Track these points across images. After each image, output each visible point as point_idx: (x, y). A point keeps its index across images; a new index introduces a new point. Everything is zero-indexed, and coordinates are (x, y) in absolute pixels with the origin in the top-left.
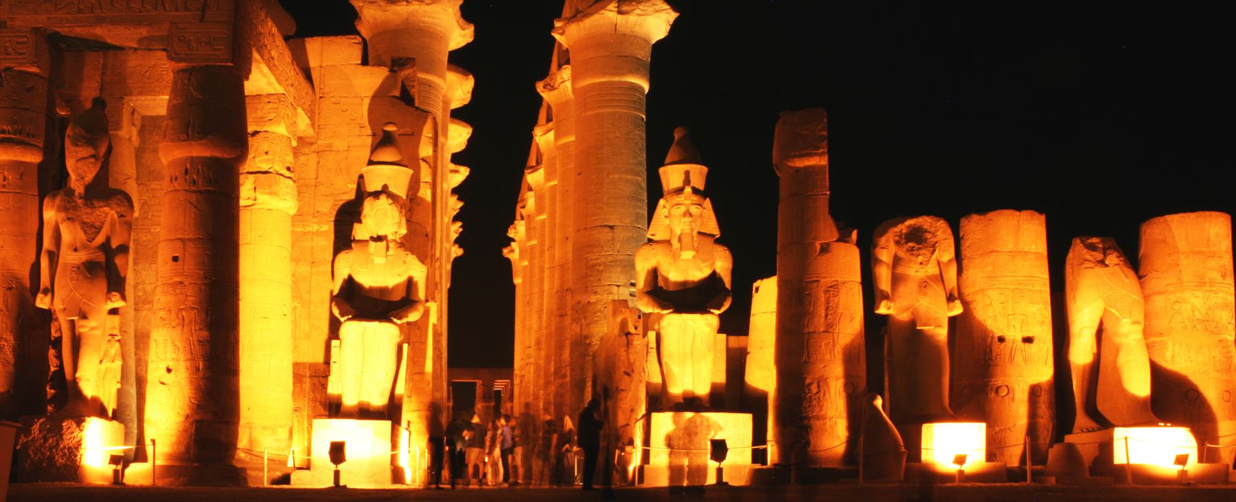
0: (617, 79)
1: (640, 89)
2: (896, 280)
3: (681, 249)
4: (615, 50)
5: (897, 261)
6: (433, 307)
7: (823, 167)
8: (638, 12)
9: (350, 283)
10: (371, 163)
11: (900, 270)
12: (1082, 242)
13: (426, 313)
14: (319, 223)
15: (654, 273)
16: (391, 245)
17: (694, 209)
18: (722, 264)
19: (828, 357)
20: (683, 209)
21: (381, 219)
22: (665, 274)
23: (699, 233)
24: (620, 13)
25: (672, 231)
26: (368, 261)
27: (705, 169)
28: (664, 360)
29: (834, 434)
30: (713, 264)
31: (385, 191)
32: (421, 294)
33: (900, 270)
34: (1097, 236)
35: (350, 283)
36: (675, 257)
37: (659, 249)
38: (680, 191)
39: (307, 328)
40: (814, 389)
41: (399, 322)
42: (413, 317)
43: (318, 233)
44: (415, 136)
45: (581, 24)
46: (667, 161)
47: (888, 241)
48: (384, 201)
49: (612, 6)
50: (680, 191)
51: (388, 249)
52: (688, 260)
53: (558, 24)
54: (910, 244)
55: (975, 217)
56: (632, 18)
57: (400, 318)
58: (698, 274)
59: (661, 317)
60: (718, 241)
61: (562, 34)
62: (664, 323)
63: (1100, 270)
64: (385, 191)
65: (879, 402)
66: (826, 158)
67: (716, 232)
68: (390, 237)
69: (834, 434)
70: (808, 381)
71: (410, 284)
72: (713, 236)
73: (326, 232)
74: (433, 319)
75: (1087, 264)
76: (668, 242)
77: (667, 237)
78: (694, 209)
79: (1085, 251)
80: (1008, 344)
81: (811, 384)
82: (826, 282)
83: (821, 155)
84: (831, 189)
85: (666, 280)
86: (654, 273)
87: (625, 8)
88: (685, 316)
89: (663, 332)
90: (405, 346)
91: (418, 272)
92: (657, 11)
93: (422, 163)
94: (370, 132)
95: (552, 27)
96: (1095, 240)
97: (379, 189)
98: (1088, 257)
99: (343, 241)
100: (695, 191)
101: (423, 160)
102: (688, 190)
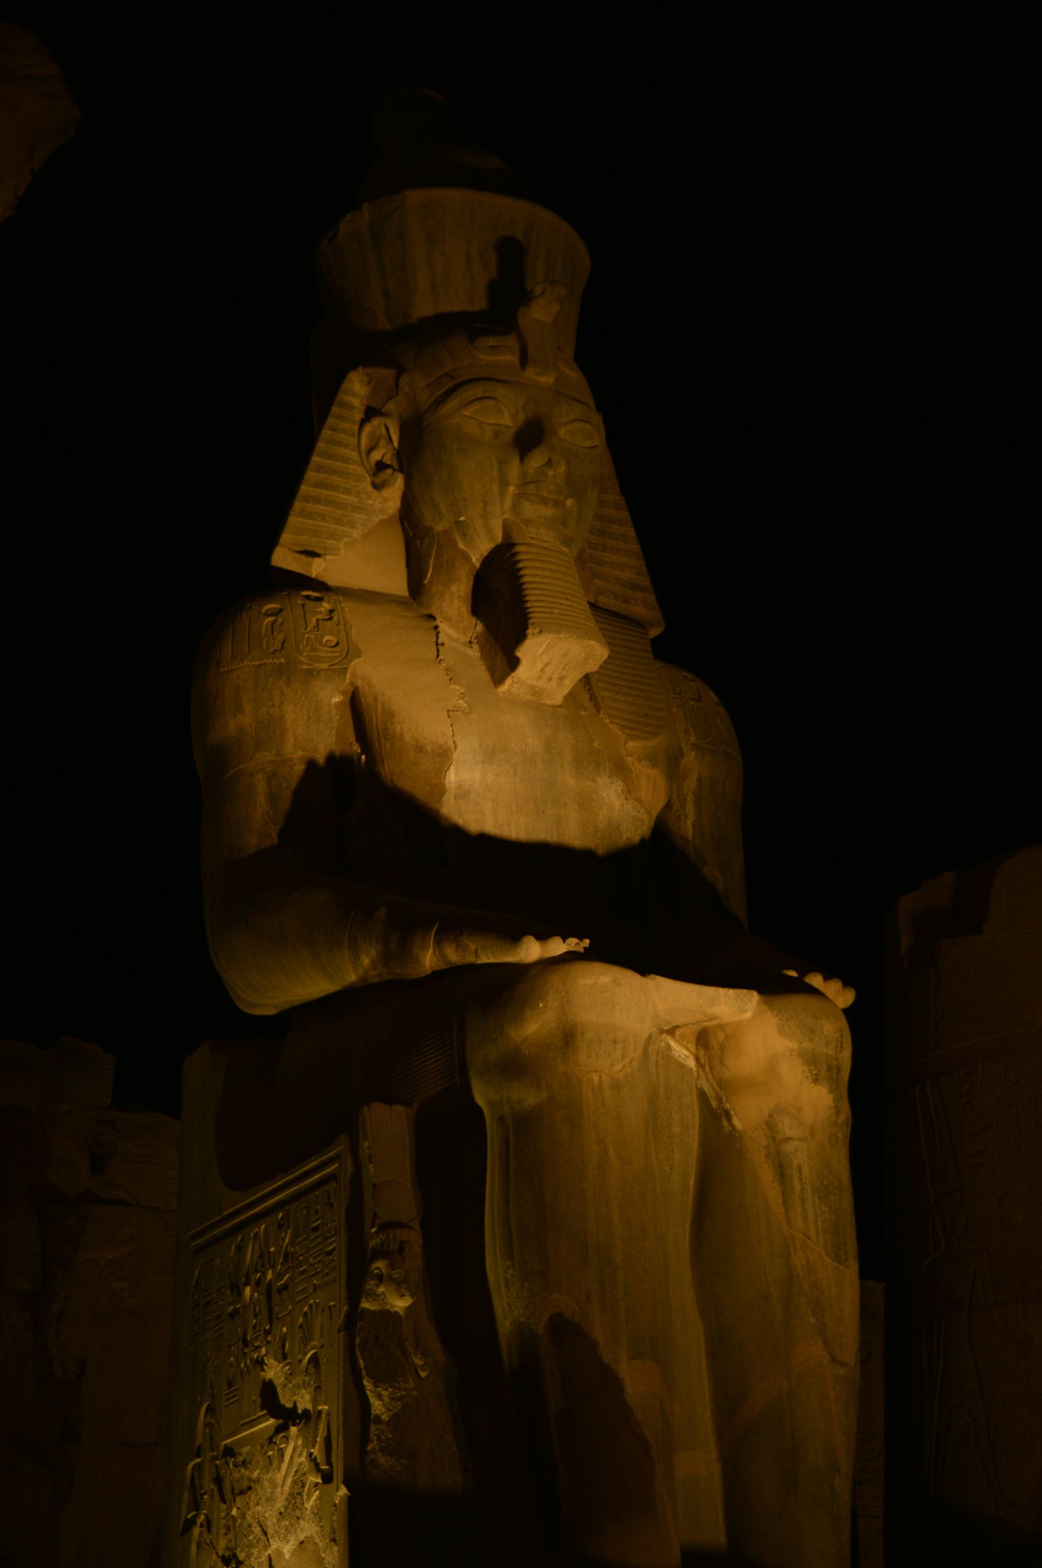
60: (664, 650)
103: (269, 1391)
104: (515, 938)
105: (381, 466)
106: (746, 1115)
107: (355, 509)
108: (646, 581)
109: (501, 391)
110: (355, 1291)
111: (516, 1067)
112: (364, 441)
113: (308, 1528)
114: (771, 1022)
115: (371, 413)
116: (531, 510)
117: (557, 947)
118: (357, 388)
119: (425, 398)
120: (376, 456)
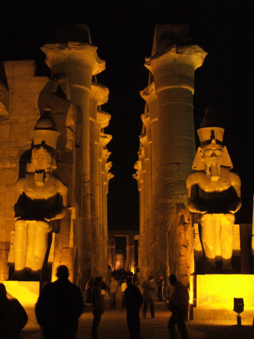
0: (177, 87)
1: (190, 92)
3: (211, 175)
4: (175, 72)
6: (73, 210)
8: (187, 52)
9: (23, 198)
10: (36, 129)
13: (70, 213)
14: (11, 163)
16: (47, 175)
17: (217, 153)
18: (235, 182)
20: (211, 152)
21: (41, 161)
22: (203, 189)
23: (221, 166)
24: (177, 53)
26: (33, 186)
27: (223, 130)
28: (204, 241)
31: (43, 144)
32: (65, 203)
35: (23, 198)
36: (209, 180)
37: (198, 175)
38: (209, 142)
39: (4, 223)
41: (48, 220)
42: (58, 217)
43: (10, 169)
44: (63, 115)
45: (158, 59)
48: (42, 150)
49: (173, 49)
50: (209, 142)
51: (45, 177)
52: (215, 182)
53: (147, 60)
56: (184, 55)
57: (49, 218)
58: (223, 188)
59: (200, 216)
60: (232, 171)
61: (149, 65)
62: (203, 219)
64: (43, 144)
67: (231, 165)
68: (46, 171)
71: (58, 197)
72: (229, 167)
73: (14, 168)
74: (73, 217)
76: (203, 172)
77: (203, 168)
78: (217, 153)
86: (196, 188)
87: (180, 51)
88: (215, 215)
89: (202, 225)
90: (54, 234)
91: (62, 190)
92: (196, 52)
93: (68, 130)
94: (39, 112)
95: (144, 62)
97: (40, 143)
99: (23, 173)
100: (218, 142)
101: (69, 127)
102: (214, 141)
104: (201, 211)
105: (202, 157)
106: (222, 224)
107: (200, 161)
108: (231, 162)
109: (209, 151)
112: (200, 154)
114: (224, 216)
115: (201, 151)
116: (213, 163)
117: (205, 212)
120: (202, 155)
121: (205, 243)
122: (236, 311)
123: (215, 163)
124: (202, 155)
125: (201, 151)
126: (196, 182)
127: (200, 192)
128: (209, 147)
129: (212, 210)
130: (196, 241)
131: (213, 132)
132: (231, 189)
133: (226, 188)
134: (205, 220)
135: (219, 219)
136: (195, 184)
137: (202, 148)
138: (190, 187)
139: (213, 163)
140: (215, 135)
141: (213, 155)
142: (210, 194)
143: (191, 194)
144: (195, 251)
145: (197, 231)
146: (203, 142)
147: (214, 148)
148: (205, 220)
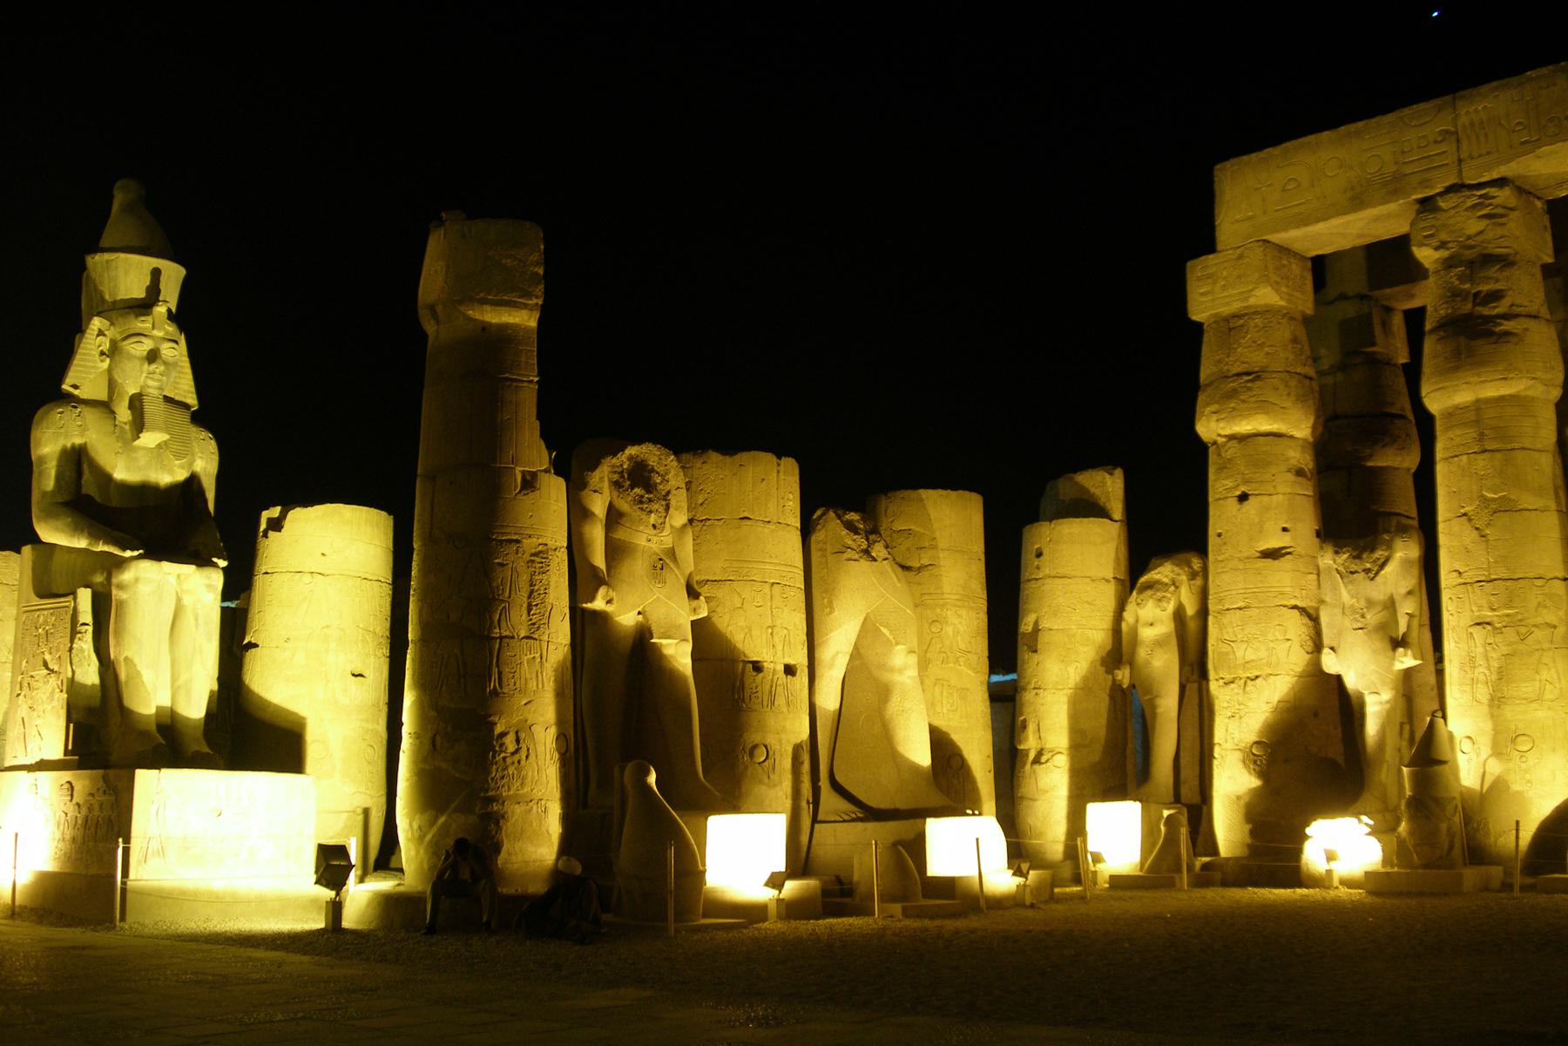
2: (615, 551)
5: (614, 517)
7: (527, 330)
11: (620, 534)
12: (839, 517)
15: (77, 459)
17: (167, 350)
18: (202, 460)
19: (532, 685)
20: (148, 345)
25: (112, 385)
27: (182, 272)
29: (537, 835)
30: (191, 464)
33: (620, 534)
34: (856, 511)
37: (90, 414)
40: (510, 742)
46: (104, 243)
47: (601, 479)
50: (143, 306)
54: (637, 491)
55: (715, 457)
58: (169, 475)
59: (114, 565)
60: (198, 419)
62: (127, 576)
63: (864, 564)
65: (652, 778)
66: (537, 315)
67: (192, 400)
69: (537, 835)
70: (498, 729)
75: (850, 554)
79: (845, 532)
80: (766, 676)
81: (503, 735)
82: (529, 545)
83: (531, 308)
84: (539, 374)
85: (108, 478)
86: (77, 459)
96: (853, 516)
98: (850, 543)
103: (46, 665)
104: (124, 549)
105: (102, 353)
106: (187, 601)
110: (72, 641)
111: (121, 587)
113: (55, 703)
115: (101, 333)
116: (150, 383)
117: (136, 553)
118: (97, 323)
119: (119, 337)
121: (126, 659)
122: (327, 886)
123: (156, 384)
124: (106, 347)
125: (101, 333)
126: (78, 441)
127: (87, 476)
128: (143, 324)
129: (159, 550)
130: (82, 650)
131: (156, 274)
132: (193, 481)
133: (181, 476)
134: (137, 580)
135: (173, 580)
136: (73, 447)
137: (112, 324)
138: (56, 456)
139: (150, 383)
140: (162, 286)
141: (153, 356)
142: (125, 487)
143: (58, 478)
144: (73, 687)
145: (86, 615)
146: (115, 302)
147: (161, 334)
148: (137, 580)
